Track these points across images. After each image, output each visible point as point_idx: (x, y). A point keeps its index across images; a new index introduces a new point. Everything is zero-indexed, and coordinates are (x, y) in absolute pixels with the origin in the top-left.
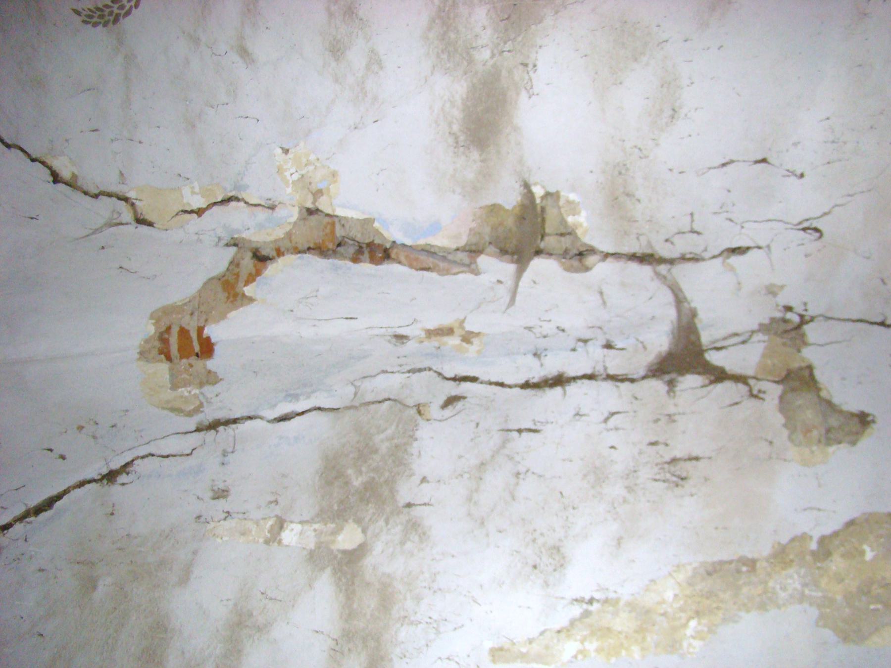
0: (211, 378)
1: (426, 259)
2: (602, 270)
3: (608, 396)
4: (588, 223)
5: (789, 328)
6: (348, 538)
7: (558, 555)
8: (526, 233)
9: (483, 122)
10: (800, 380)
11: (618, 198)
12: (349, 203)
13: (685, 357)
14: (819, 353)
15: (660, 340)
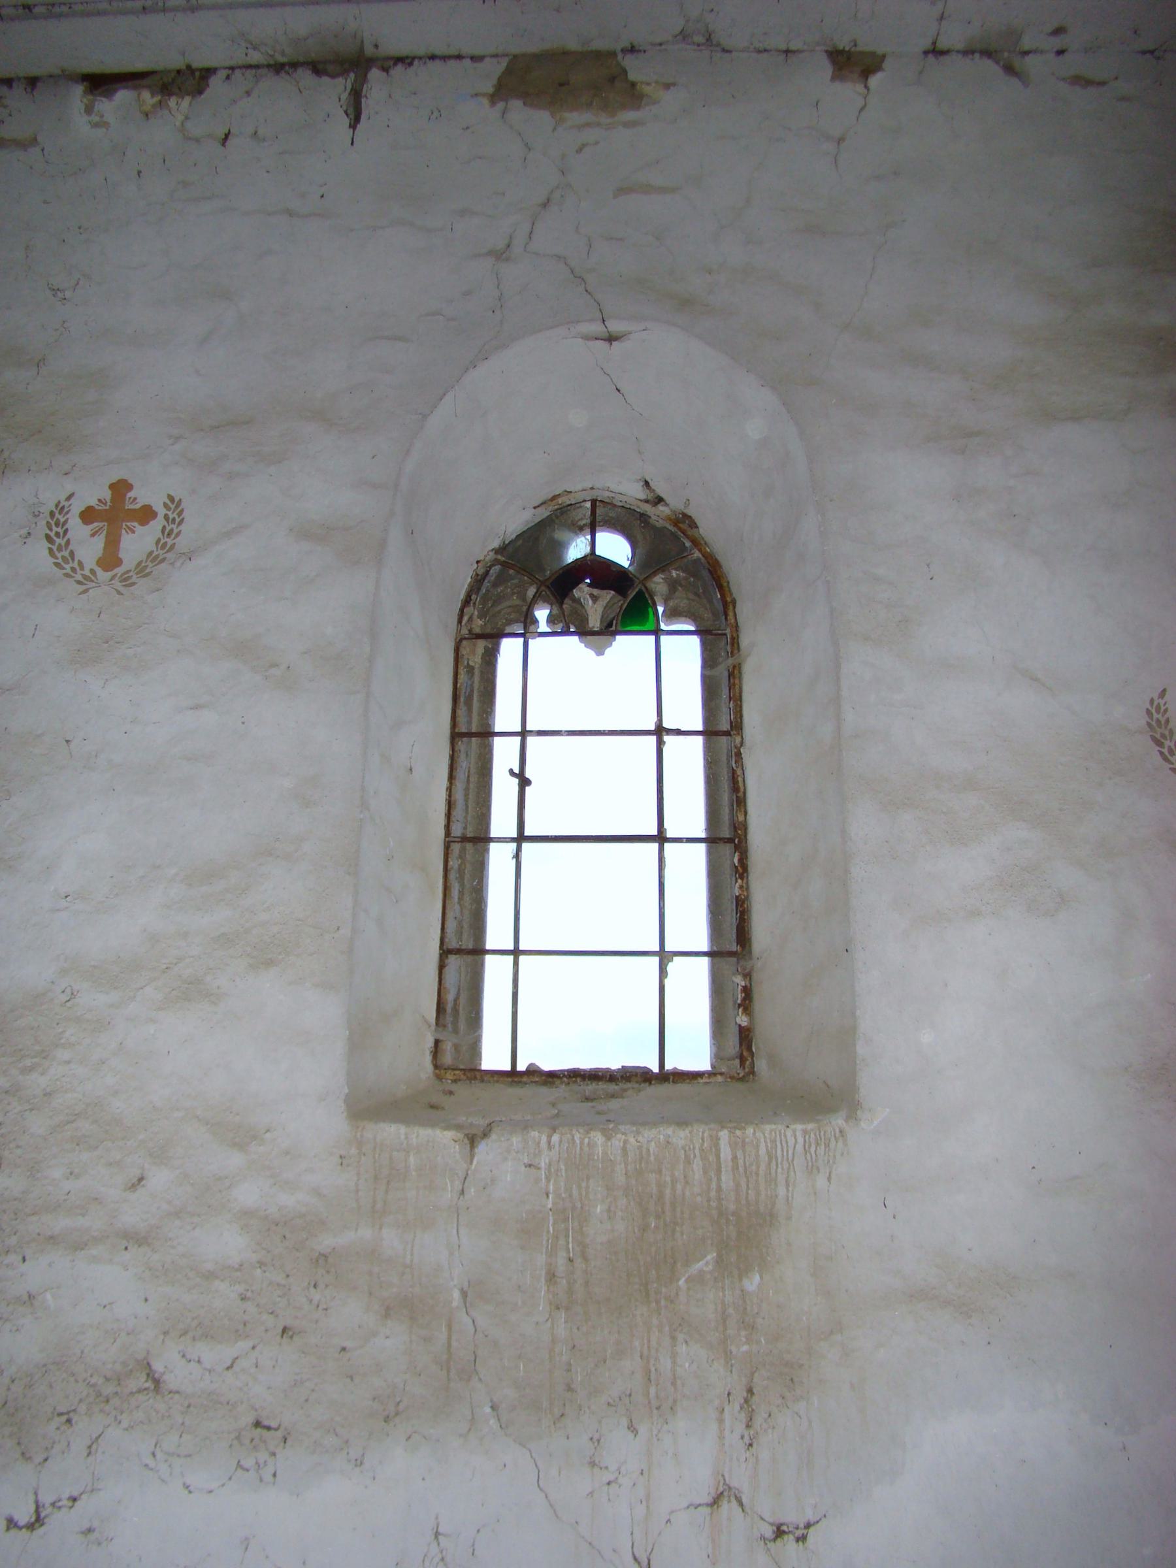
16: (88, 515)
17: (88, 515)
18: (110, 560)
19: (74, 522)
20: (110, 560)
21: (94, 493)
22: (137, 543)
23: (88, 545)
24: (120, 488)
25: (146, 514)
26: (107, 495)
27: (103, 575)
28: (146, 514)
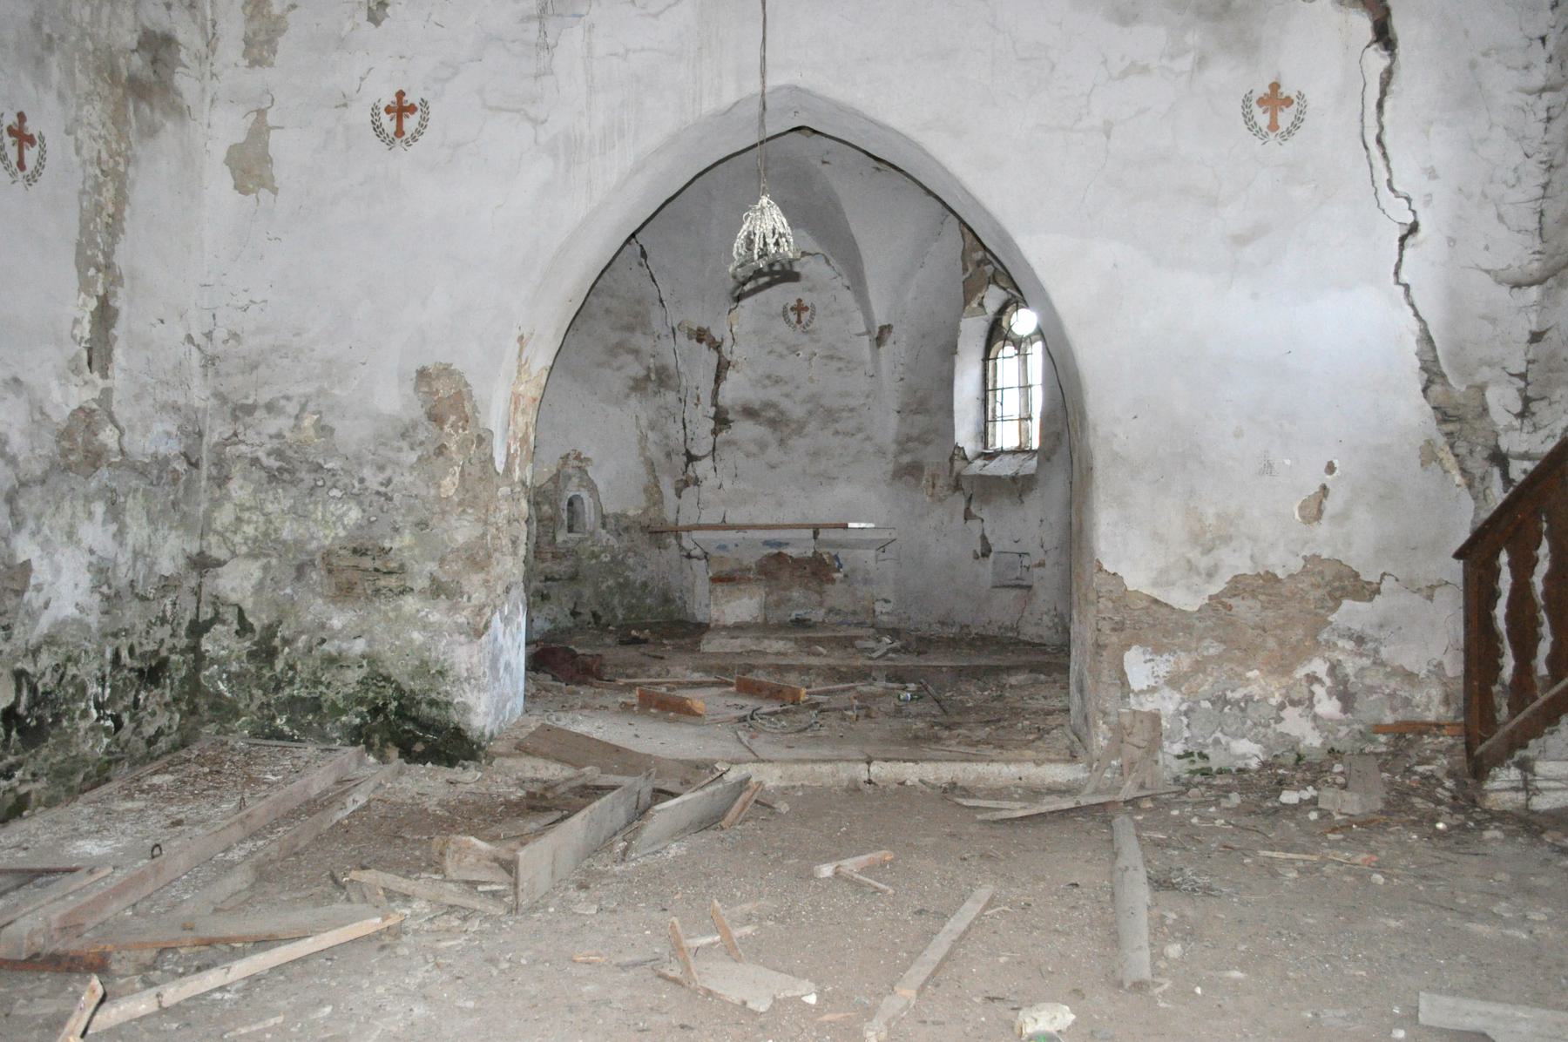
0: (690, 338)
1: (715, 393)
2: (711, 438)
3: (682, 440)
4: (723, 435)
5: (697, 482)
6: (653, 376)
7: (652, 429)
8: (721, 420)
9: (749, 412)
10: (687, 484)
11: (730, 443)
12: (731, 374)
13: (691, 458)
14: (692, 489)
15: (694, 452)
16: (1261, 102)
17: (1261, 102)
18: (1273, 126)
19: (1255, 107)
20: (1273, 126)
21: (1262, 89)
22: (1285, 118)
23: (1263, 119)
24: (1275, 86)
25: (1288, 102)
26: (1268, 91)
27: (1272, 135)
28: (1288, 102)
